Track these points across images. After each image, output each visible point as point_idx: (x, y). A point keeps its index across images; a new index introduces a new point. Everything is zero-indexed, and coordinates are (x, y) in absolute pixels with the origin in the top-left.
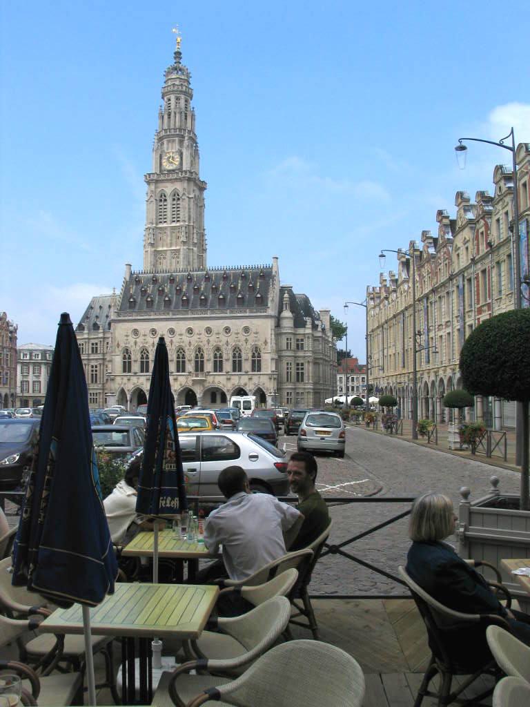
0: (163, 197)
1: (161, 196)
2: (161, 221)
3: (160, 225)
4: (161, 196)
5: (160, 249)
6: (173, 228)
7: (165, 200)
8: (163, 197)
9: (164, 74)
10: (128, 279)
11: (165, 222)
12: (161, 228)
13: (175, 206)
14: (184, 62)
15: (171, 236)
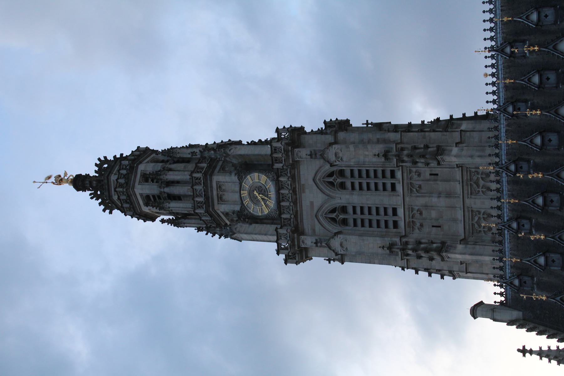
0: (334, 215)
1: (333, 220)
2: (391, 224)
3: (402, 224)
4: (333, 220)
5: (460, 228)
6: (411, 188)
7: (344, 209)
8: (334, 215)
9: (108, 211)
10: (516, 314)
11: (395, 211)
12: (410, 225)
13: (357, 186)
14: (91, 171)
15: (430, 193)
